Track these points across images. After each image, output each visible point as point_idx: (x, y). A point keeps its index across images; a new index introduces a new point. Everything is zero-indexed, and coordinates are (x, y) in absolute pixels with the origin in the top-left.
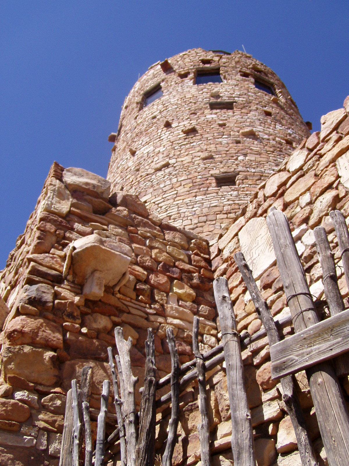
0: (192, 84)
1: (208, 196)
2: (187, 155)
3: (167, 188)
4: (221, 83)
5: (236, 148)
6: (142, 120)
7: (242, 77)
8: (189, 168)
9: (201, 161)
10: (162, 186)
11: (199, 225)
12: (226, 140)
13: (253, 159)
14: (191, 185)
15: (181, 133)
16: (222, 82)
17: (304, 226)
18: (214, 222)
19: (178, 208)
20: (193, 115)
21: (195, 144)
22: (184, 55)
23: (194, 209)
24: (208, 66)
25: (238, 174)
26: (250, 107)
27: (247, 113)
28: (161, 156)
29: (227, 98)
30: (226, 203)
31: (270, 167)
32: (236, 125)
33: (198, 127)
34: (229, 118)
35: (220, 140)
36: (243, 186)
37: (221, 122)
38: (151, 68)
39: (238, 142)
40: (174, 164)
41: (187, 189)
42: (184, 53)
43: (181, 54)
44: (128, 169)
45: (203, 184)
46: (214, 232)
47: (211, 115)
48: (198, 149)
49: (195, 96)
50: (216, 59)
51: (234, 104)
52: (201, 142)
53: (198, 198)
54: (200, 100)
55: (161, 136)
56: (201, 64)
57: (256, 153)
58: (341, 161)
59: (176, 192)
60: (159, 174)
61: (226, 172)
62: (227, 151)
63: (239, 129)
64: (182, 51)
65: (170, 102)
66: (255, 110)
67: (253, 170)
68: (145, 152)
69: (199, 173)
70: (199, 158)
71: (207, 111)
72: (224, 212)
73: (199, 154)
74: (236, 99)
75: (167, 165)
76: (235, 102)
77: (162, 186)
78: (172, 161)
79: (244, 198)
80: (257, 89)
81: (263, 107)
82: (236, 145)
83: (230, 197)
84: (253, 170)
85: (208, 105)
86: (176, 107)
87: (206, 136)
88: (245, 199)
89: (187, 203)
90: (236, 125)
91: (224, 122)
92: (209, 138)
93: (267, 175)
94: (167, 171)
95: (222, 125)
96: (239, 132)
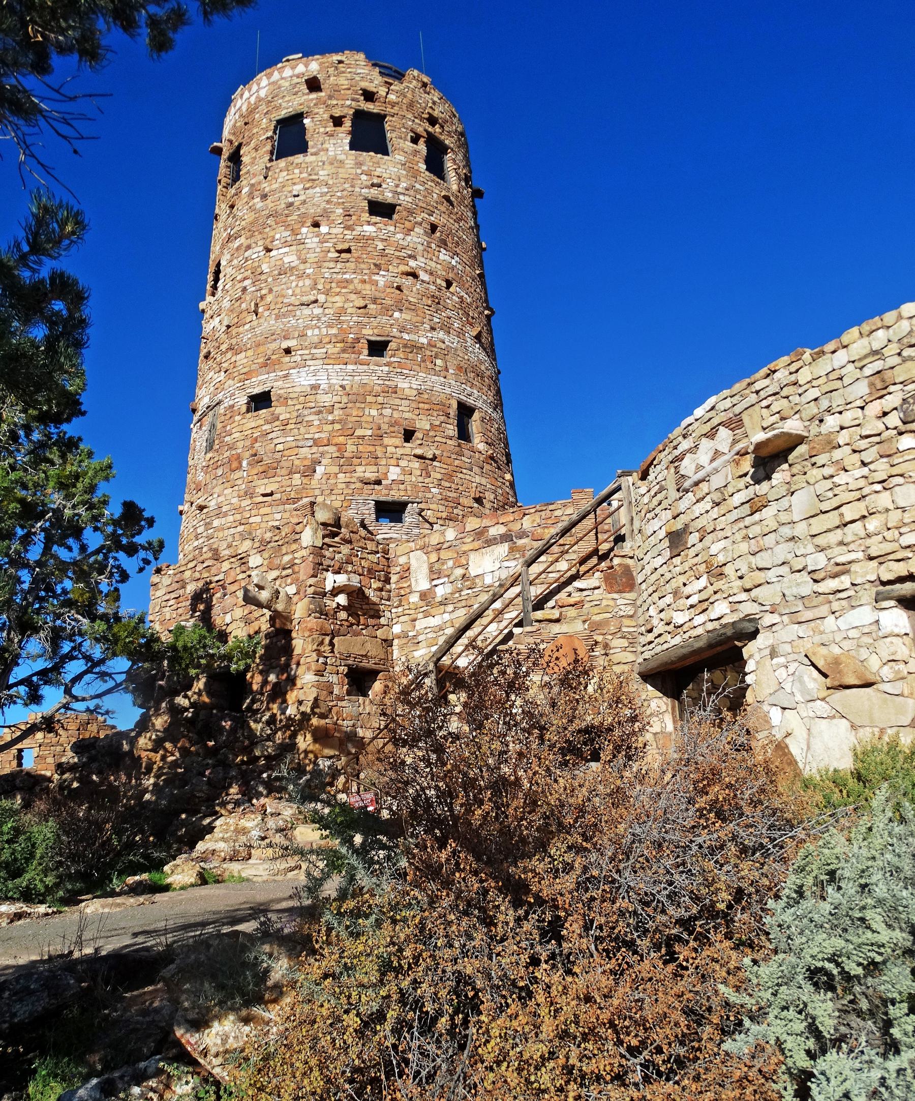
0: (348, 148)
1: (360, 367)
3: (316, 340)
4: (386, 157)
6: (276, 186)
9: (354, 310)
11: (350, 405)
13: (408, 318)
15: (332, 250)
16: (388, 155)
17: (446, 579)
18: (363, 405)
22: (340, 62)
23: (344, 383)
29: (390, 195)
35: (376, 278)
36: (395, 359)
38: (288, 61)
41: (336, 350)
43: (336, 57)
44: (263, 277)
47: (371, 227)
50: (382, 91)
53: (350, 367)
55: (306, 241)
56: (362, 98)
58: (472, 556)
59: (324, 350)
60: (307, 311)
65: (317, 174)
66: (421, 224)
67: (406, 336)
68: (286, 260)
71: (366, 216)
74: (401, 197)
75: (316, 301)
76: (400, 205)
78: (322, 298)
80: (427, 173)
81: (429, 215)
85: (365, 204)
86: (326, 190)
87: (363, 266)
92: (365, 271)
94: (317, 311)
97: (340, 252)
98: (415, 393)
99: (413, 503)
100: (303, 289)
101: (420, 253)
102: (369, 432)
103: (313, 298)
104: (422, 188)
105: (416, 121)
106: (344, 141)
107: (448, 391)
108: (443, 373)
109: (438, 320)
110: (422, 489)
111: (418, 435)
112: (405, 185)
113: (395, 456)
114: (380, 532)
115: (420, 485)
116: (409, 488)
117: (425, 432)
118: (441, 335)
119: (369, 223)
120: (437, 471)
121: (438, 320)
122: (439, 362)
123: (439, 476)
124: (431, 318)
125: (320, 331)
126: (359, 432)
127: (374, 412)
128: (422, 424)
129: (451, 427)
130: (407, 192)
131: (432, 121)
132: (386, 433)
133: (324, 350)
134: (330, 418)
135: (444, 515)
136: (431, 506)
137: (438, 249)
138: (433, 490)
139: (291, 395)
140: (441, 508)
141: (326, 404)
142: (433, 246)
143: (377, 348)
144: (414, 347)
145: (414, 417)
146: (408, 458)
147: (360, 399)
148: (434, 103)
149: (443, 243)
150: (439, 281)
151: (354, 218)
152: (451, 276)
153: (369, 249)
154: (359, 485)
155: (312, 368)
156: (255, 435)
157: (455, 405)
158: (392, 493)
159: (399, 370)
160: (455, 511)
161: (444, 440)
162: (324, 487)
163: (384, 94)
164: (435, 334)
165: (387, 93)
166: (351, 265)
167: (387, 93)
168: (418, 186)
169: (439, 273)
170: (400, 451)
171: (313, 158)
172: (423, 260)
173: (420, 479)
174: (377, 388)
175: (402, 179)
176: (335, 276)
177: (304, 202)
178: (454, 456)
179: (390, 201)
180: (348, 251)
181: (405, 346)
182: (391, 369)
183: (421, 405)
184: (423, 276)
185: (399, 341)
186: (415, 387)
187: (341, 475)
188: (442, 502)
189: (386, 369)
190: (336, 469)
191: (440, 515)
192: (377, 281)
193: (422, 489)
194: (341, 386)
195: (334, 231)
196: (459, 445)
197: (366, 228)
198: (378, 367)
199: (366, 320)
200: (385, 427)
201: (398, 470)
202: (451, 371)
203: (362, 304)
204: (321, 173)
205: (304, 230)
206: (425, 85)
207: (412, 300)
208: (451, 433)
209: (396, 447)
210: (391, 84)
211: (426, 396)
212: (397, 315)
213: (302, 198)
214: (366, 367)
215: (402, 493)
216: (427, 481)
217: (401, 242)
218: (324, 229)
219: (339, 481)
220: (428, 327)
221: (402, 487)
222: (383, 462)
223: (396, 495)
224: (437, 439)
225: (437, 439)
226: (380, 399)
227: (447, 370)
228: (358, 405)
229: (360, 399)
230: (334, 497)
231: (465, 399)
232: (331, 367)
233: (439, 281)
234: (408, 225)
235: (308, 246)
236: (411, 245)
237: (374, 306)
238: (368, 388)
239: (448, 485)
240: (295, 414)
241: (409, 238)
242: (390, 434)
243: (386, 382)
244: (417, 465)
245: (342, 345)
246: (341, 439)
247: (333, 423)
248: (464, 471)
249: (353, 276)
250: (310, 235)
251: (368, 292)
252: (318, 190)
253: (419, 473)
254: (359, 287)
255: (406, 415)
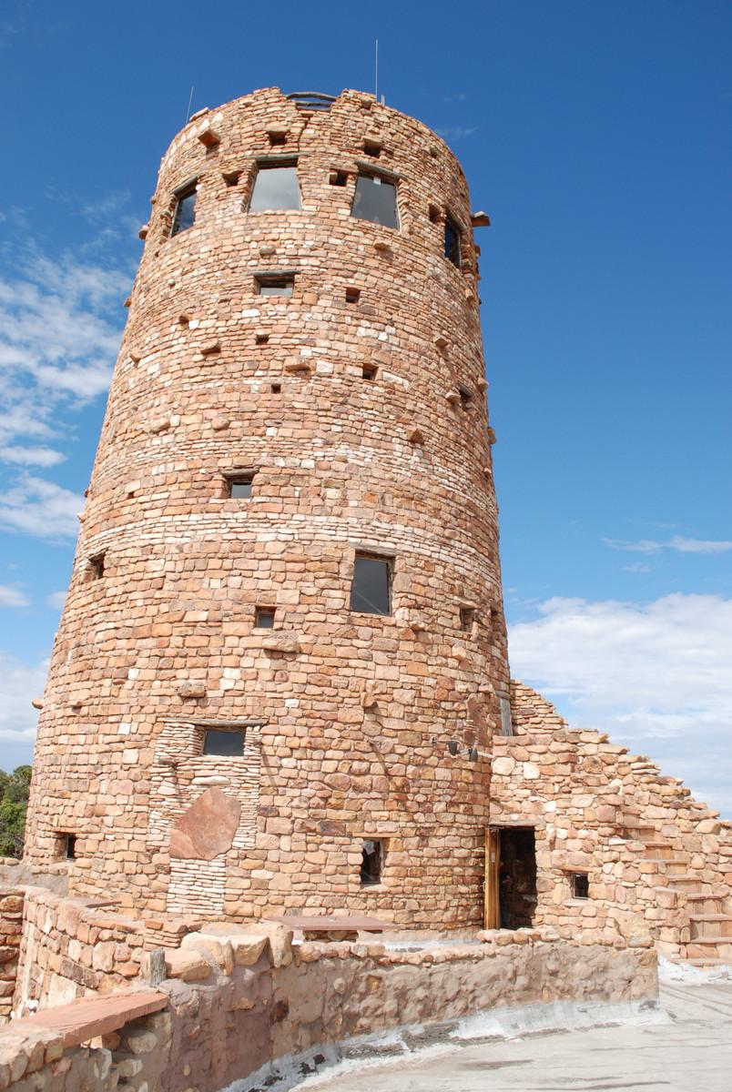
0: (238, 211)
1: (207, 516)
2: (195, 412)
3: (159, 480)
5: (268, 404)
7: (331, 187)
8: (194, 446)
10: (154, 471)
11: (184, 575)
12: (259, 382)
13: (287, 433)
14: (188, 486)
18: (201, 574)
19: (165, 531)
20: (223, 304)
21: (210, 385)
22: (247, 105)
23: (184, 540)
24: (277, 151)
25: (258, 472)
26: (321, 286)
27: (312, 305)
28: (164, 399)
29: (286, 261)
30: (225, 537)
31: (311, 453)
32: (285, 341)
33: (224, 341)
34: (277, 320)
35: (250, 381)
37: (261, 332)
38: (194, 119)
39: (276, 389)
40: (177, 427)
41: (182, 493)
42: (246, 101)
45: (204, 487)
46: (200, 594)
48: (213, 400)
49: (237, 247)
51: (296, 276)
52: (220, 383)
53: (194, 517)
54: (243, 263)
56: (268, 143)
57: (298, 417)
59: (166, 495)
60: (156, 441)
61: (241, 467)
62: (255, 412)
63: (285, 352)
64: (244, 95)
66: (328, 293)
67: (281, 462)
69: (204, 459)
70: (208, 425)
71: (248, 297)
72: (220, 555)
73: (213, 413)
74: (303, 261)
75: (166, 427)
76: (298, 273)
77: (154, 471)
78: (174, 421)
79: (253, 527)
80: (352, 220)
82: (270, 396)
83: (233, 523)
84: (281, 462)
86: (204, 271)
88: (254, 530)
89: (177, 526)
90: (285, 341)
91: (268, 331)
92: (235, 375)
93: (301, 472)
94: (167, 439)
95: (262, 340)
96: (283, 361)
97: (206, 353)
98: (282, 546)
99: (253, 726)
100: (159, 410)
101: (323, 333)
102: (203, 616)
103: (162, 422)
104: (339, 242)
105: (343, 154)
106: (237, 202)
107: (341, 535)
108: (337, 510)
109: (339, 429)
110: (270, 702)
111: (279, 615)
112: (311, 243)
113: (236, 651)
114: (197, 773)
115: (268, 695)
116: (249, 701)
117: (290, 608)
118: (342, 450)
119: (252, 306)
120: (299, 672)
121: (339, 429)
122: (332, 493)
123: (303, 678)
124: (326, 427)
125: (166, 468)
126: (190, 617)
127: (216, 584)
128: (286, 597)
129: (339, 594)
130: (312, 253)
131: (372, 149)
132: (227, 616)
133: (166, 495)
134: (158, 594)
135: (304, 742)
136: (283, 730)
137: (355, 322)
138: (289, 703)
139: (124, 562)
140: (301, 731)
141: (155, 575)
142: (348, 320)
143: (238, 481)
144: (294, 476)
145: (277, 586)
146: (256, 653)
147: (200, 564)
148: (379, 125)
149: (369, 314)
150: (350, 369)
151: (232, 303)
152: (372, 359)
153: (245, 343)
154: (176, 700)
155: (149, 521)
156: (83, 616)
157: (350, 556)
158: (222, 711)
159: (262, 515)
160: (327, 733)
161: (322, 617)
162: (133, 702)
163: (298, 131)
164: (330, 451)
165: (303, 129)
166: (219, 369)
167: (303, 129)
168: (332, 241)
169: (353, 356)
170: (245, 642)
171: (198, 232)
172: (327, 343)
173: (270, 686)
174: (226, 546)
175: (308, 237)
176: (196, 386)
177: (179, 291)
178: (337, 641)
179: (286, 269)
180: (216, 350)
181: (277, 476)
182: (251, 515)
183: (290, 566)
184: (324, 367)
185: (267, 470)
186: (282, 537)
187: (157, 683)
188: (304, 721)
189: (243, 515)
190: (151, 674)
191: (295, 742)
192: (249, 387)
193: (270, 702)
194: (178, 547)
195: (204, 324)
196: (350, 622)
197: (246, 313)
198: (235, 510)
199: (226, 445)
200: (226, 605)
201: (236, 673)
202: (352, 503)
203: (219, 422)
204: (202, 250)
205: (173, 328)
206: (367, 106)
207: (296, 405)
208: (337, 604)
209: (240, 637)
210: (310, 116)
211: (299, 550)
212: (270, 432)
213: (177, 286)
214: (214, 515)
215: (237, 711)
216: (279, 688)
217: (294, 324)
218: (193, 324)
219: (153, 692)
220: (319, 442)
221: (238, 701)
222: (216, 661)
223: (225, 714)
224: (309, 617)
225: (309, 617)
226: (228, 564)
227: (344, 501)
228: (195, 573)
229: (200, 564)
230: (142, 718)
231: (375, 543)
232: (169, 518)
233: (350, 369)
234: (308, 298)
235: (173, 350)
236: (308, 325)
237: (240, 424)
238: (212, 547)
239: (317, 690)
240: (121, 590)
241: (306, 316)
242: (233, 617)
243: (240, 536)
244: (266, 663)
245: (188, 486)
246: (166, 629)
247: (161, 600)
248: (353, 663)
249: (220, 383)
250: (178, 334)
251: (235, 404)
252: (195, 273)
253: (269, 676)
254: (224, 398)
255: (263, 584)
